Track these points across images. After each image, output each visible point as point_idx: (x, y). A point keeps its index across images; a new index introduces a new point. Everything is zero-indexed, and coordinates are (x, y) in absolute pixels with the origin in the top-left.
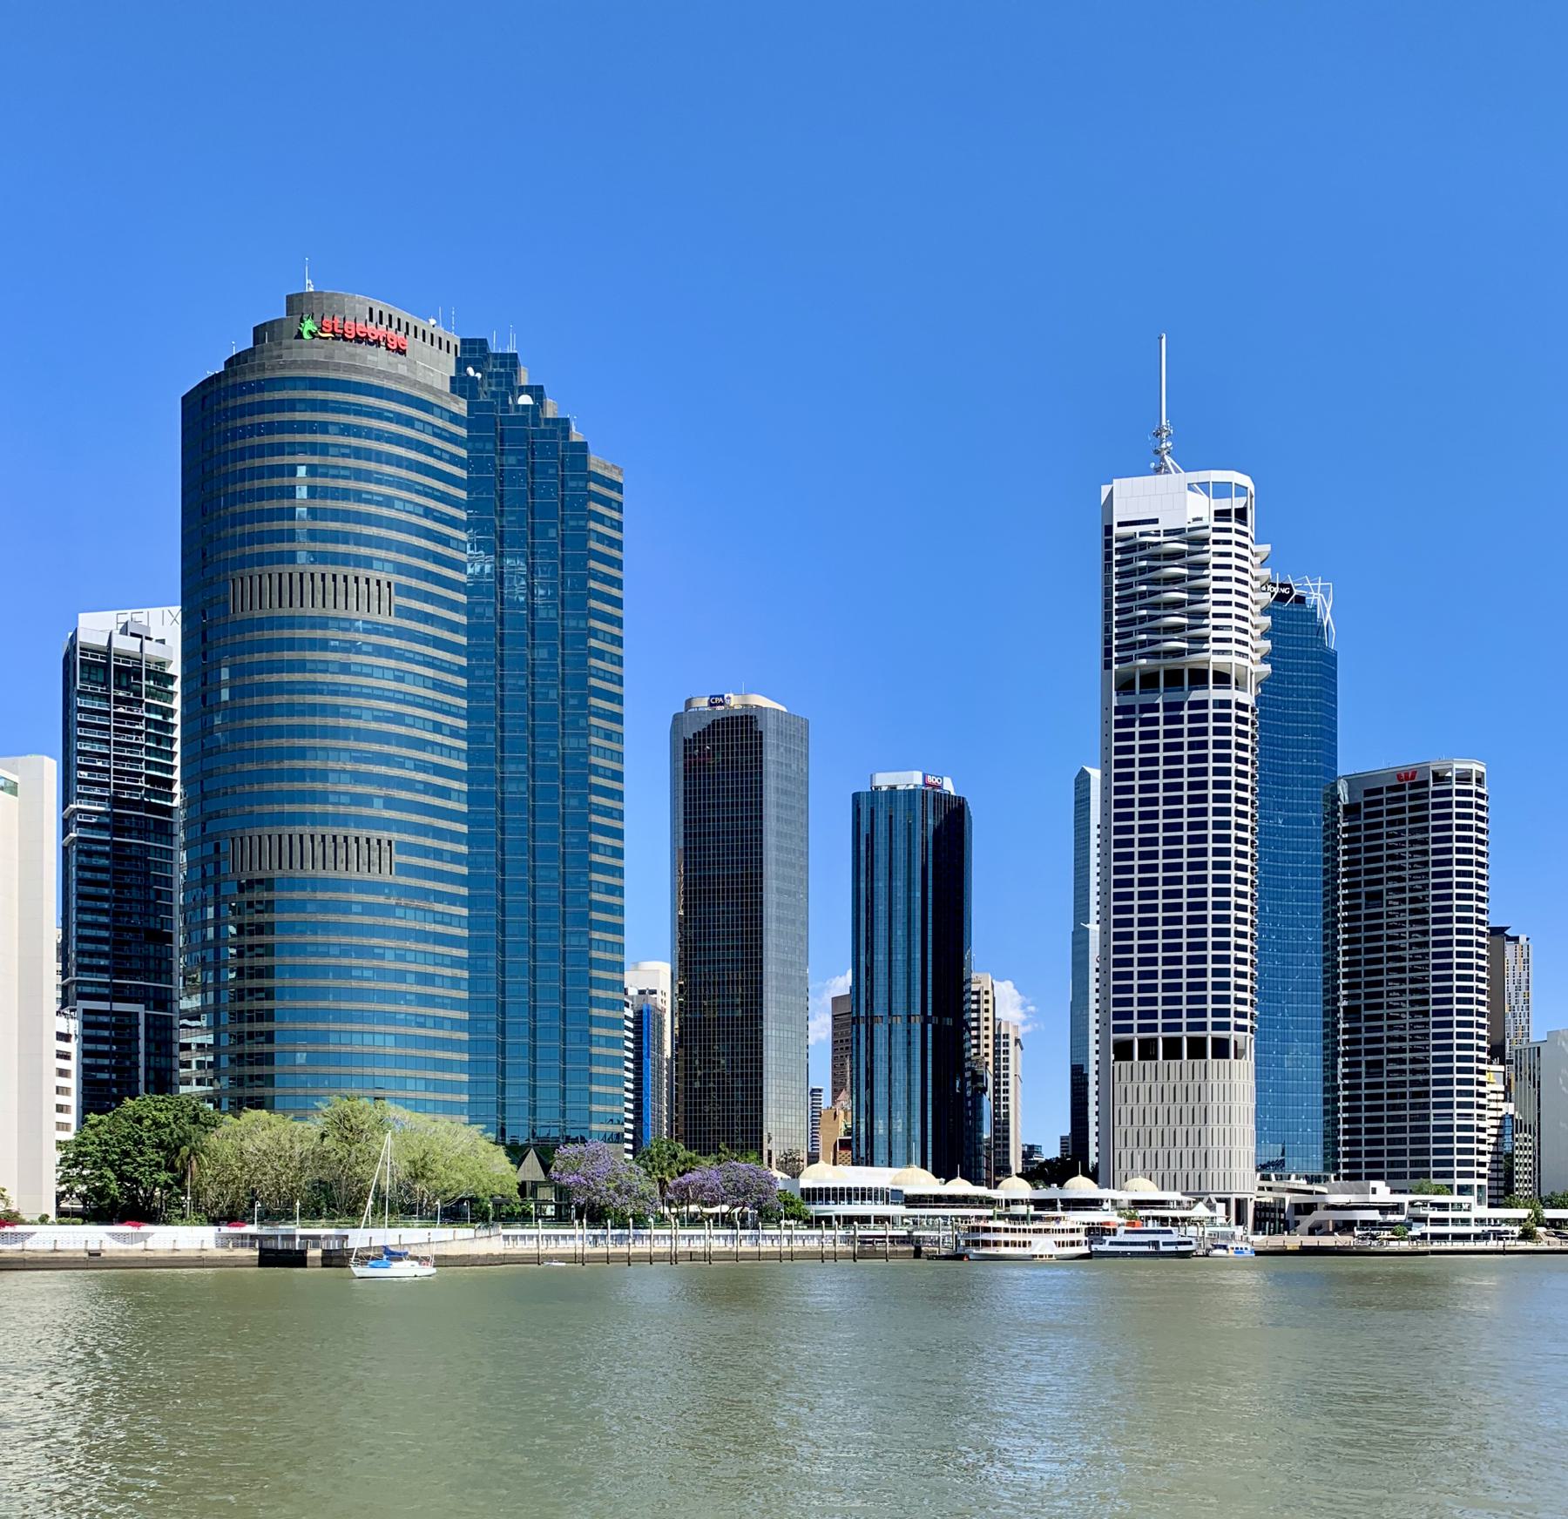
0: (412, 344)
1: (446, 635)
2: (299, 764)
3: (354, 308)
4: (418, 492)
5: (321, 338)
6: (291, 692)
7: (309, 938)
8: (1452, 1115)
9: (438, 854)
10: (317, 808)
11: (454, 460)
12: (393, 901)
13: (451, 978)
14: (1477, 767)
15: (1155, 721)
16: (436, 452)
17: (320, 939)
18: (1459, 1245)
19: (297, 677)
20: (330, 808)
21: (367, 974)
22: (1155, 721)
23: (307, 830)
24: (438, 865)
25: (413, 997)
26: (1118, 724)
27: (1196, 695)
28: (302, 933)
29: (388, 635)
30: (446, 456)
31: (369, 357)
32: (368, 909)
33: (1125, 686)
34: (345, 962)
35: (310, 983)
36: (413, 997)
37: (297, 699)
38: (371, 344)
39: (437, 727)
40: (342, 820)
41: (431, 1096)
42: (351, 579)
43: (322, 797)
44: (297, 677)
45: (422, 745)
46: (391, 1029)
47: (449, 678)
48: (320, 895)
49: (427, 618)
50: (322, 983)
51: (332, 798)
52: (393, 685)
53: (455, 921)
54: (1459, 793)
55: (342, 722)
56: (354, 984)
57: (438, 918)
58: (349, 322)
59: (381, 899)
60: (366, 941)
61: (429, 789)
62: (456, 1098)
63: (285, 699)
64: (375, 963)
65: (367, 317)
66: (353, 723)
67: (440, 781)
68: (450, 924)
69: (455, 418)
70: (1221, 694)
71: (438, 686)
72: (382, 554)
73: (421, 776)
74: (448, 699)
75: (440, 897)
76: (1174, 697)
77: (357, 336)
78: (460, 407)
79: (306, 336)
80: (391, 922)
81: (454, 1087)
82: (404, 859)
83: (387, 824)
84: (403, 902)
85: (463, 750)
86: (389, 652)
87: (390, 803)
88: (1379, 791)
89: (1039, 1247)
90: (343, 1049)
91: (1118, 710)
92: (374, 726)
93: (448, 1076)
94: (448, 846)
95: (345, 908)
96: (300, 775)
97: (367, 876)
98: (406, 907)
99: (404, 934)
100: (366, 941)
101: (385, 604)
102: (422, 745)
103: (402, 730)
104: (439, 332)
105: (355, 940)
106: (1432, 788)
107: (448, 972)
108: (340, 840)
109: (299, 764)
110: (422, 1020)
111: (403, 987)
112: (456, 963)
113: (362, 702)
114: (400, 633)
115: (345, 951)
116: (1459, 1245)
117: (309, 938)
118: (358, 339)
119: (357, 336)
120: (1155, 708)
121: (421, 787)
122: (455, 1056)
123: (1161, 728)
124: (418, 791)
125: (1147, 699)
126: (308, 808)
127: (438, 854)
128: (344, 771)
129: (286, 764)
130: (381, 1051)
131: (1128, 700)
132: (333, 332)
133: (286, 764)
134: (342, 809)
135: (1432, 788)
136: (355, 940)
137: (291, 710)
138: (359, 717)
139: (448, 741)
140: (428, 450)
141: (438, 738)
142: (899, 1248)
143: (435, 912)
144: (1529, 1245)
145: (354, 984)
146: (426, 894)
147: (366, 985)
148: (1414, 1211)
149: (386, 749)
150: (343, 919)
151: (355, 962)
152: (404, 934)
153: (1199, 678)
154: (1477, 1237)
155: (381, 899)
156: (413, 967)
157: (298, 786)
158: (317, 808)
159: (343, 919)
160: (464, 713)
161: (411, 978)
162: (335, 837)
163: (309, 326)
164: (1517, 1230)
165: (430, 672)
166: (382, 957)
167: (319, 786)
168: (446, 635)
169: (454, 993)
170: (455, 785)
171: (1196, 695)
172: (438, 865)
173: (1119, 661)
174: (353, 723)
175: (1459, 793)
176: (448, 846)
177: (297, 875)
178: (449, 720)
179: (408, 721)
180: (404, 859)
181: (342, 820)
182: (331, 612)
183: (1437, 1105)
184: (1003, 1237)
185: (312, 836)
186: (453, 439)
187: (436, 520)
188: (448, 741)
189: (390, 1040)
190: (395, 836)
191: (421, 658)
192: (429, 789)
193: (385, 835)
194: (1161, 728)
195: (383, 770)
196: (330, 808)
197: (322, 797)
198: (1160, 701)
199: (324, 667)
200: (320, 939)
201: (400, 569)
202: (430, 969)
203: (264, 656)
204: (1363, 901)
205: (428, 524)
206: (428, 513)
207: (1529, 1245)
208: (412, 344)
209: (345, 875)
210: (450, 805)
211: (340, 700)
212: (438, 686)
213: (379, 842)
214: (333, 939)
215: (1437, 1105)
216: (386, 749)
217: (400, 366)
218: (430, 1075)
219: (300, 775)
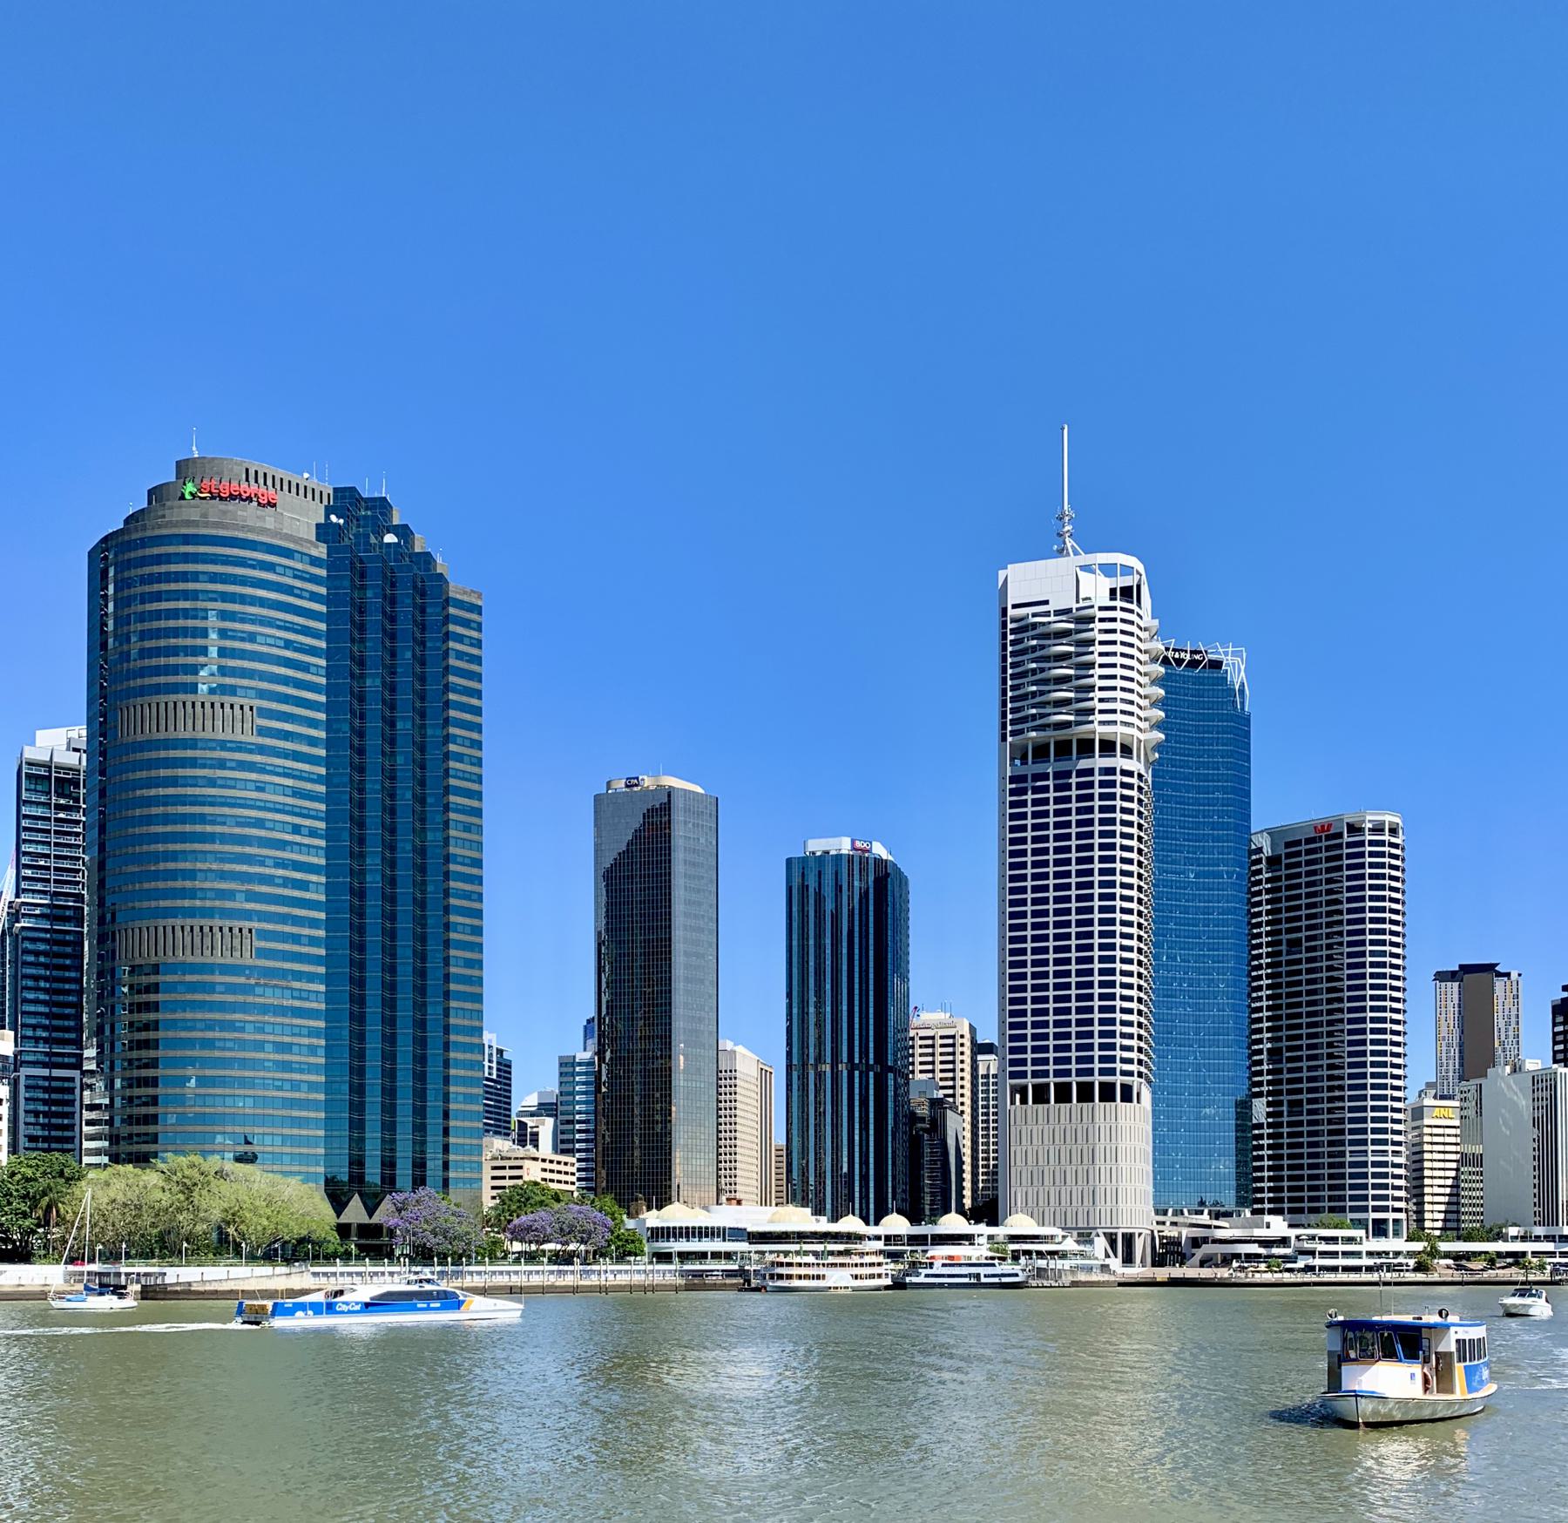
0: (282, 498)
1: (305, 749)
2: (171, 866)
3: (232, 469)
4: (279, 627)
5: (201, 498)
6: (165, 804)
7: (179, 1015)
8: (1366, 1151)
9: (296, 939)
10: (187, 903)
11: (314, 597)
12: (252, 981)
13: (309, 1046)
14: (1389, 818)
15: (1046, 789)
16: (296, 591)
17: (189, 1015)
18: (1353, 1277)
19: (171, 791)
20: (198, 903)
21: (229, 1044)
22: (1046, 789)
23: (178, 922)
24: (296, 948)
25: (271, 1064)
26: (1012, 792)
27: (1084, 764)
28: (174, 1011)
29: (251, 752)
30: (307, 595)
31: (239, 513)
32: (231, 989)
33: (1020, 754)
34: (209, 1035)
35: (179, 1053)
36: (271, 1064)
37: (171, 810)
38: (244, 500)
39: (296, 829)
40: (208, 913)
41: (287, 1150)
42: (217, 706)
43: (192, 894)
44: (171, 791)
45: (281, 845)
46: (251, 1092)
47: (309, 786)
48: (189, 978)
49: (287, 736)
50: (189, 1053)
51: (199, 894)
52: (254, 795)
53: (313, 997)
54: (1372, 843)
55: (209, 829)
56: (217, 1054)
57: (296, 994)
58: (225, 482)
59: (242, 980)
60: (228, 1017)
61: (287, 882)
62: (312, 1151)
63: (161, 810)
64: (236, 1035)
65: (244, 476)
66: (218, 829)
67: (298, 875)
68: (307, 999)
69: (315, 561)
70: (1107, 762)
71: (297, 793)
72: (245, 682)
73: (280, 872)
74: (307, 804)
75: (298, 976)
76: (1063, 766)
77: (231, 494)
78: (321, 551)
79: (188, 496)
80: (250, 999)
81: (309, 1141)
82: (263, 944)
83: (247, 915)
84: (262, 982)
85: (322, 848)
86: (251, 767)
87: (252, 897)
88: (1298, 843)
90: (207, 1110)
91: (1013, 780)
92: (237, 830)
93: (304, 1132)
94: (306, 931)
95: (210, 988)
96: (173, 875)
97: (229, 961)
98: (265, 985)
99: (265, 1009)
100: (228, 1017)
101: (248, 726)
102: (281, 845)
103: (262, 833)
104: (314, 483)
105: (217, 1016)
106: (1346, 839)
107: (306, 1041)
108: (206, 930)
109: (171, 866)
110: (280, 1083)
111: (261, 1055)
112: (313, 1033)
113: (227, 811)
114: (262, 750)
115: (210, 1026)
116: (1353, 1277)
117: (179, 1015)
118: (232, 497)
119: (231, 494)
120: (1045, 777)
121: (281, 881)
122: (312, 1115)
123: (1051, 795)
124: (278, 885)
125: (1039, 768)
126: (179, 903)
127: (296, 939)
128: (211, 870)
129: (162, 866)
130: (241, 1111)
131: (1022, 770)
132: (210, 492)
133: (162, 866)
134: (208, 904)
135: (1346, 839)
136: (217, 1016)
137: (167, 819)
138: (224, 824)
139: (307, 841)
140: (289, 590)
141: (298, 839)
142: (728, 1281)
143: (292, 989)
144: (1420, 1277)
145: (217, 1054)
146: (284, 974)
147: (228, 1054)
148: (1299, 1244)
149: (248, 850)
150: (207, 998)
151: (217, 1035)
152: (265, 1009)
153: (1086, 747)
154: (1369, 1269)
155: (242, 980)
156: (271, 1038)
157: (170, 884)
158: (187, 903)
159: (207, 998)
160: (323, 815)
161: (268, 1047)
162: (201, 928)
163: (190, 488)
164: (1412, 1262)
165: (289, 782)
166: (242, 1030)
167: (188, 884)
168: (305, 749)
169: (312, 1060)
170: (314, 878)
171: (1084, 764)
172: (296, 948)
173: (1013, 733)
174: (218, 829)
175: (1372, 843)
176: (306, 931)
177: (170, 961)
178: (308, 822)
179: (268, 824)
180: (263, 944)
181: (208, 913)
182: (201, 735)
183: (1352, 1143)
185: (182, 927)
186: (314, 579)
187: (296, 650)
188: (307, 841)
189: (250, 1102)
190: (255, 925)
191: (281, 770)
192: (287, 882)
193: (247, 924)
194: (1051, 795)
195: (244, 868)
196: (198, 903)
197: (192, 894)
198: (1050, 770)
199: (194, 782)
200: (189, 1015)
201: (262, 694)
202: (287, 1039)
203: (144, 774)
204: (1284, 948)
205: (289, 654)
206: (288, 644)
207: (1420, 1277)
208: (282, 498)
209: (210, 960)
210: (307, 895)
211: (207, 810)
212: (297, 793)
213: (241, 930)
214: (199, 1016)
215: (1352, 1143)
216: (248, 850)
217: (269, 519)
218: (287, 1131)
219: (173, 875)
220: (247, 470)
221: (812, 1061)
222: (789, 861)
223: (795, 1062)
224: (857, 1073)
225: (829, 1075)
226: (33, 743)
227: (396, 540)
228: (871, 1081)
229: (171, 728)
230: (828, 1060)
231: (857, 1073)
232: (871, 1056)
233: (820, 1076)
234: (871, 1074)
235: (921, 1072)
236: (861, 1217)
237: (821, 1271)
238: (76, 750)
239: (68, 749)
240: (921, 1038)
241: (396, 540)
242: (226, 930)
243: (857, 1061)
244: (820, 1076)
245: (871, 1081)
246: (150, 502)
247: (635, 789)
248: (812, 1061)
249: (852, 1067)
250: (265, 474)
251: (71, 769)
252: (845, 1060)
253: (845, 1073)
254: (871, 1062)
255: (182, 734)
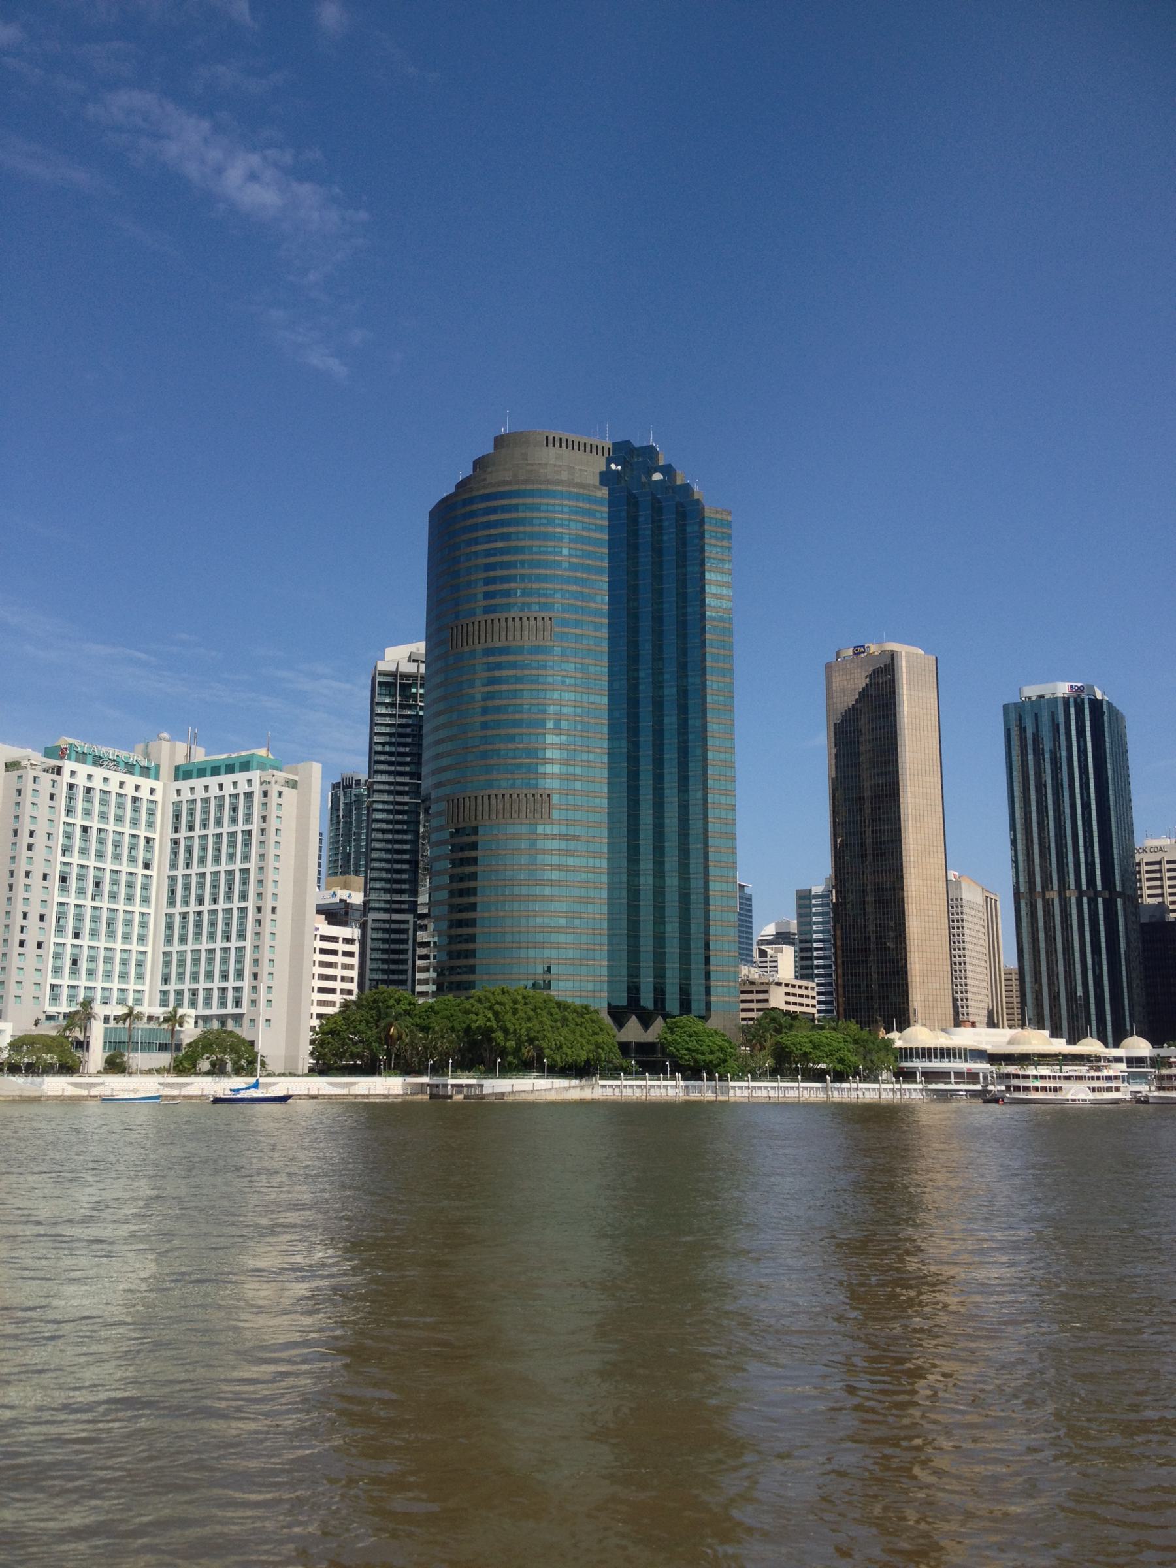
31: (542, 471)
89: (1072, 1092)
184: (1032, 1083)
220: (547, 437)
221: (1039, 889)
222: (1006, 708)
223: (1022, 890)
224: (1085, 899)
225: (1056, 901)
226: (383, 659)
227: (662, 477)
228: (1101, 906)
229: (489, 640)
230: (1056, 887)
231: (1085, 899)
232: (1099, 882)
233: (1048, 904)
234: (1100, 900)
235: (1150, 896)
236: (1099, 1039)
237: (1057, 1084)
238: (415, 661)
239: (409, 661)
240: (1148, 864)
241: (662, 477)
242: (530, 796)
243: (1084, 887)
244: (1048, 904)
245: (1101, 906)
246: (475, 469)
247: (862, 655)
248: (1039, 889)
249: (1081, 894)
250: (561, 439)
251: (411, 676)
252: (1073, 887)
253: (1073, 901)
254: (1099, 888)
255: (497, 644)
